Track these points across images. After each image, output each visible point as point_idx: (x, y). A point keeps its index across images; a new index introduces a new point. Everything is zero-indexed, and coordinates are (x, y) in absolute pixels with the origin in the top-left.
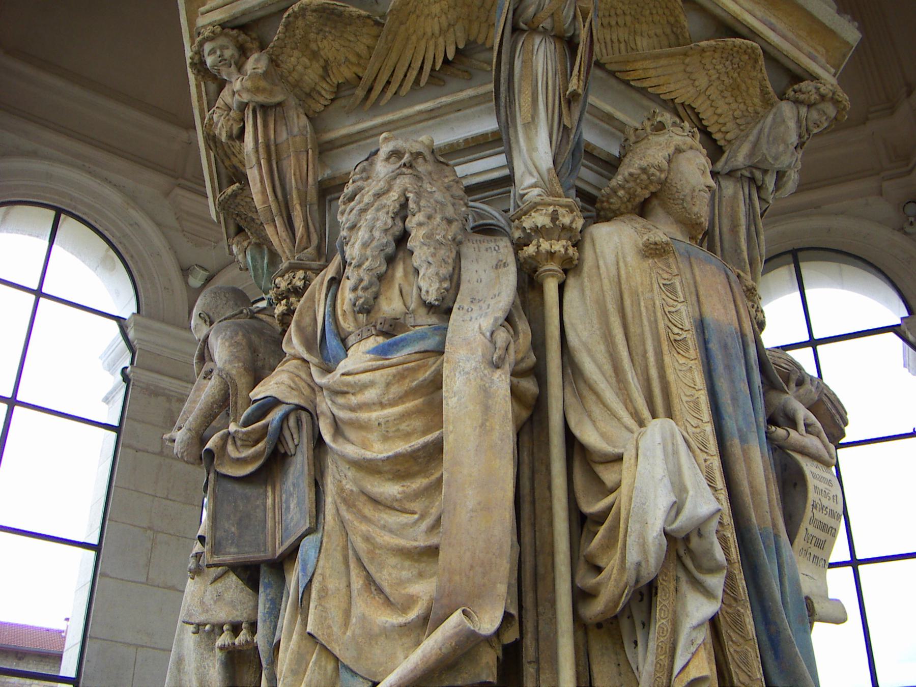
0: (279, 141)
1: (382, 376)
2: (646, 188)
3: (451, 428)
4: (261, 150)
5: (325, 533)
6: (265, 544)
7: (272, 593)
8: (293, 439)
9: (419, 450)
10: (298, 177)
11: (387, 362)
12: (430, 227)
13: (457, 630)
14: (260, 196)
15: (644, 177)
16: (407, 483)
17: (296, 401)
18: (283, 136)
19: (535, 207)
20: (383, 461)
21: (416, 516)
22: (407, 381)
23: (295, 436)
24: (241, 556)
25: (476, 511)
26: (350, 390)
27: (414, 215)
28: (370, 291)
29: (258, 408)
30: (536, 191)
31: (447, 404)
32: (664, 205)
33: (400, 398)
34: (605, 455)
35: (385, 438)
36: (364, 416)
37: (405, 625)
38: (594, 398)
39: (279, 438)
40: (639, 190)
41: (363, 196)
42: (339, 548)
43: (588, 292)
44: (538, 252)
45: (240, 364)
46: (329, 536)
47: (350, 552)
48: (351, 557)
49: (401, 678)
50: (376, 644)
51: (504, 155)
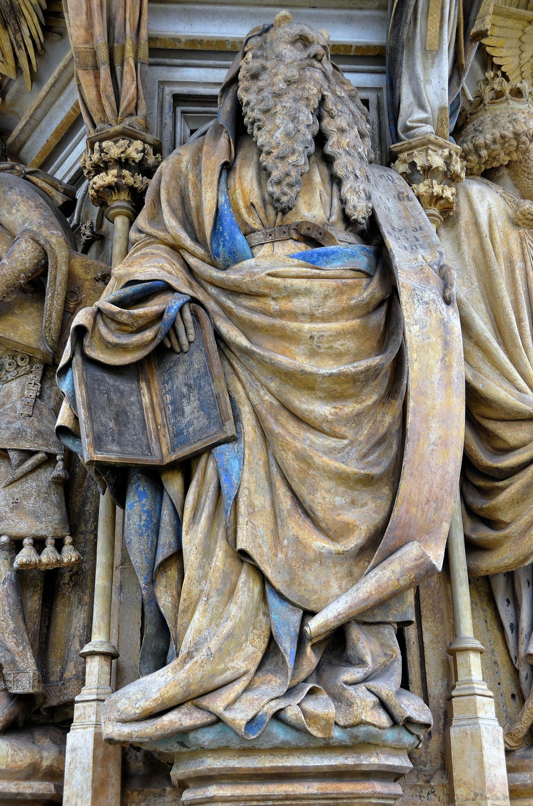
1: (321, 286)
2: (509, 154)
7: (147, 503)
9: (362, 372)
13: (419, 562)
14: (82, 32)
15: (515, 143)
16: (339, 405)
19: (425, 144)
20: (324, 376)
21: (346, 442)
22: (345, 297)
23: (191, 331)
24: (126, 456)
29: (144, 290)
30: (428, 128)
31: (410, 331)
32: (515, 177)
33: (336, 314)
34: (519, 412)
35: (313, 354)
36: (293, 325)
37: (343, 553)
38: (480, 355)
40: (503, 154)
42: (261, 463)
43: (465, 247)
47: (274, 469)
48: (279, 474)
50: (310, 570)
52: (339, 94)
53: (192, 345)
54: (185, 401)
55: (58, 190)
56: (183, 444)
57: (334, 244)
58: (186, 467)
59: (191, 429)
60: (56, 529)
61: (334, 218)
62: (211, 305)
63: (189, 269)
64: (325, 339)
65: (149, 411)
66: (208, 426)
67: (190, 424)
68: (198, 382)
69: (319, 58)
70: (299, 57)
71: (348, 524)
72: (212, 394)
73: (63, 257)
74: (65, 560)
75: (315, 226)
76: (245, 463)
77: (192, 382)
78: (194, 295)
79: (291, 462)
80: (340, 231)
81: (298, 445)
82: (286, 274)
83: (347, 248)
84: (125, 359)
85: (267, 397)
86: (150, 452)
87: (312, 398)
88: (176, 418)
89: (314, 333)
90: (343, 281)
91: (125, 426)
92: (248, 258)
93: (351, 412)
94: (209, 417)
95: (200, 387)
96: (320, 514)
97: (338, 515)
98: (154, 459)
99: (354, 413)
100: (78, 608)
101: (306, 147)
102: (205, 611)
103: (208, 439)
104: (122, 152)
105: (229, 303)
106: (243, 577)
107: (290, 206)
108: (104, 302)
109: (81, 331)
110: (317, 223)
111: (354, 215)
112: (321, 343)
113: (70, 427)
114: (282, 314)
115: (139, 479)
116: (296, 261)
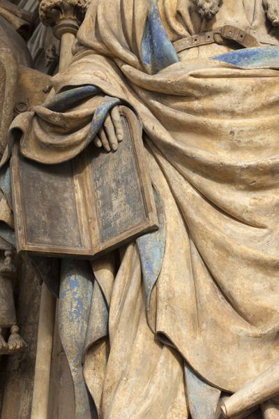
1: (240, 84)
6: (80, 239)
8: (116, 133)
16: (258, 195)
20: (242, 169)
21: (265, 231)
22: (264, 94)
23: (120, 131)
24: (56, 247)
26: (196, 93)
29: (76, 95)
33: (256, 110)
35: (234, 147)
37: (261, 336)
42: (182, 251)
49: (265, 387)
50: (228, 352)
53: (121, 143)
54: (113, 195)
55: (16, 15)
56: (110, 235)
57: (255, 45)
58: (113, 257)
59: (118, 221)
60: (3, 318)
61: (256, 22)
62: (141, 108)
63: (124, 77)
65: (82, 205)
66: (133, 219)
67: (117, 216)
68: (125, 177)
71: (266, 309)
72: (138, 188)
73: (11, 71)
74: (11, 347)
75: (236, 29)
76: (167, 251)
77: (120, 178)
78: (124, 97)
79: (211, 250)
80: (263, 34)
81: (218, 234)
82: (207, 74)
83: (268, 48)
84: (59, 158)
85: (190, 190)
86: (81, 243)
87: (233, 190)
88: (105, 212)
89: (234, 129)
90: (263, 79)
91: (57, 219)
92: (175, 62)
93: (271, 203)
94: (134, 210)
95: (127, 181)
96: (238, 299)
97: (257, 300)
98: (83, 249)
99: (274, 203)
100: (25, 392)
102: (125, 390)
103: (133, 229)
105: (157, 104)
106: (162, 358)
107: (213, 11)
108: (43, 110)
109: (17, 134)
110: (240, 27)
111: (275, 19)
112: (240, 137)
113: (6, 221)
114: (204, 112)
115: (71, 269)
116: (217, 62)
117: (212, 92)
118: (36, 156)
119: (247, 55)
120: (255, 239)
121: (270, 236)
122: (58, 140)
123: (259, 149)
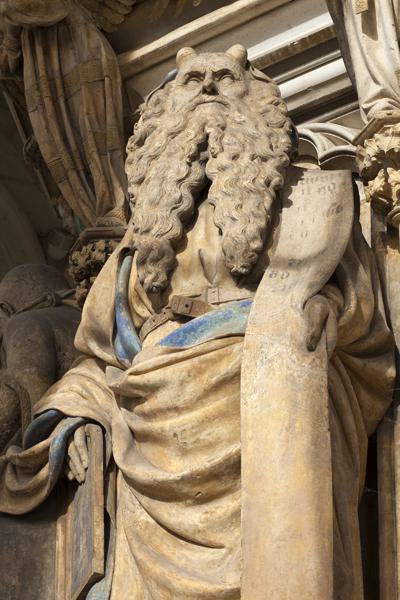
0: (67, 70)
3: (250, 433)
4: (44, 87)
5: (115, 579)
8: (81, 461)
10: (93, 116)
11: (180, 355)
12: (236, 171)
17: (85, 412)
18: (71, 63)
19: (379, 126)
20: (177, 482)
21: (224, 551)
22: (206, 376)
23: (84, 457)
25: (284, 540)
26: (141, 393)
27: (215, 157)
28: (161, 262)
30: (383, 102)
33: (200, 399)
35: (184, 452)
39: (64, 461)
41: (154, 138)
44: (387, 187)
45: (33, 370)
46: (121, 584)
51: (342, 60)
52: (238, 120)
64: (188, 433)
65: (61, 555)
69: (208, 90)
70: (188, 99)
90: (202, 357)
99: (229, 513)
101: (175, 208)
104: (87, 259)
112: (185, 438)
117: (153, 389)
118: (10, 507)
119: (193, 329)
120: (214, 564)
121: (230, 556)
122: (31, 482)
123: (210, 446)
